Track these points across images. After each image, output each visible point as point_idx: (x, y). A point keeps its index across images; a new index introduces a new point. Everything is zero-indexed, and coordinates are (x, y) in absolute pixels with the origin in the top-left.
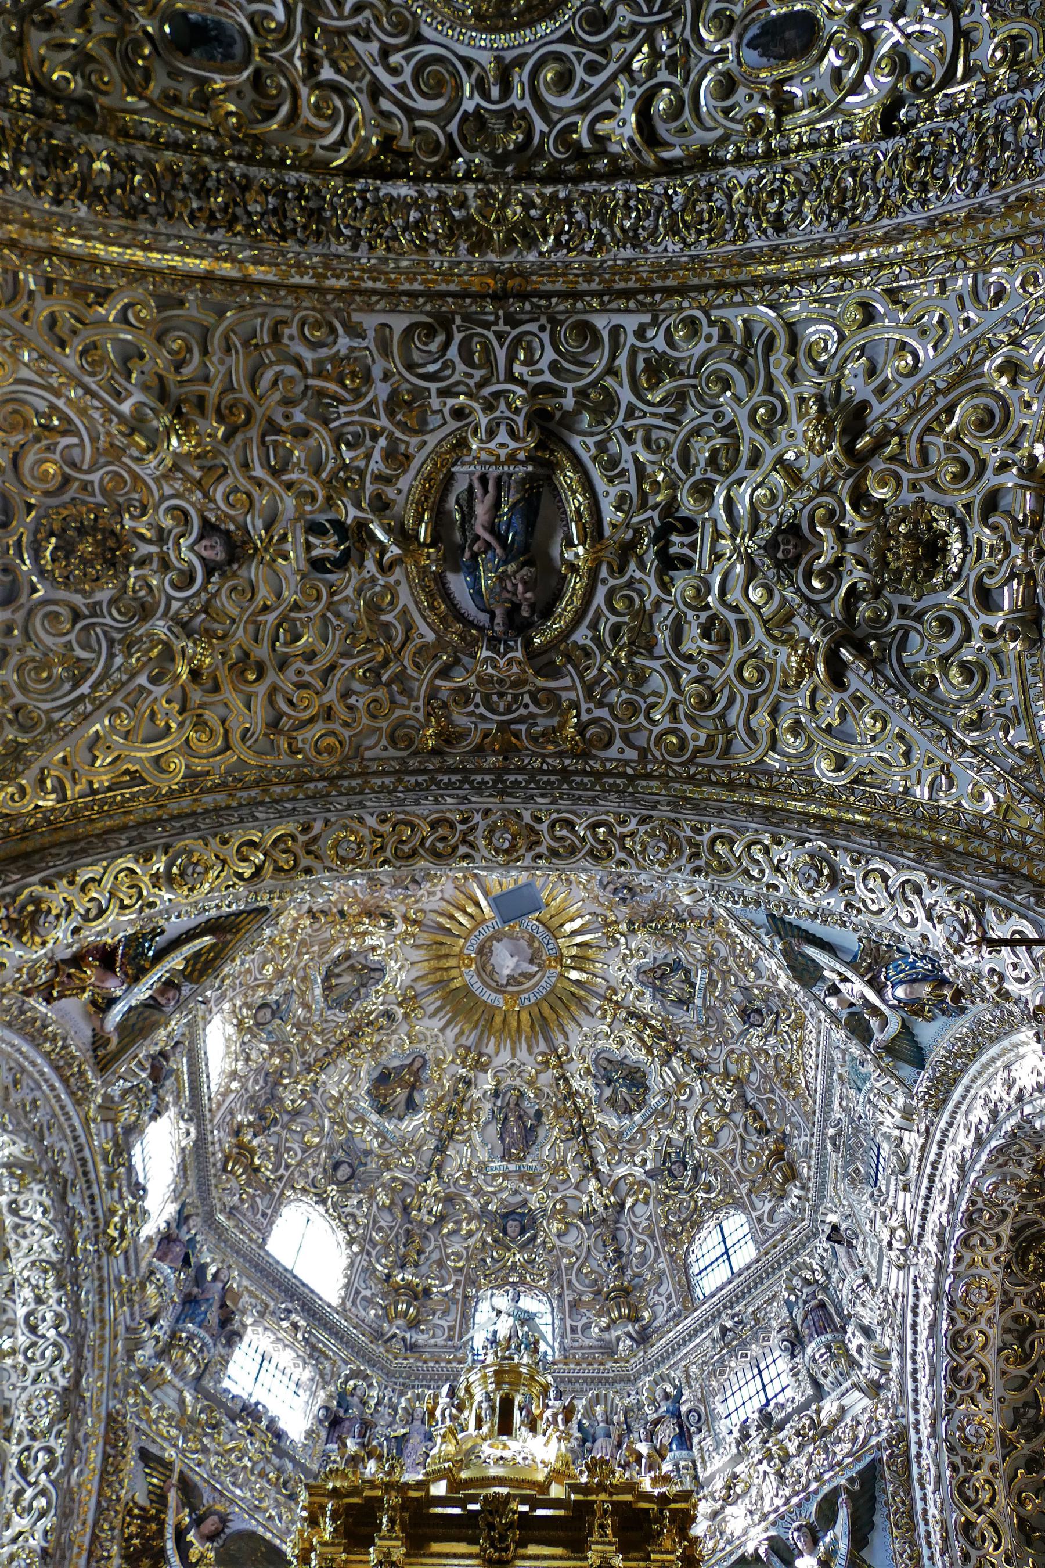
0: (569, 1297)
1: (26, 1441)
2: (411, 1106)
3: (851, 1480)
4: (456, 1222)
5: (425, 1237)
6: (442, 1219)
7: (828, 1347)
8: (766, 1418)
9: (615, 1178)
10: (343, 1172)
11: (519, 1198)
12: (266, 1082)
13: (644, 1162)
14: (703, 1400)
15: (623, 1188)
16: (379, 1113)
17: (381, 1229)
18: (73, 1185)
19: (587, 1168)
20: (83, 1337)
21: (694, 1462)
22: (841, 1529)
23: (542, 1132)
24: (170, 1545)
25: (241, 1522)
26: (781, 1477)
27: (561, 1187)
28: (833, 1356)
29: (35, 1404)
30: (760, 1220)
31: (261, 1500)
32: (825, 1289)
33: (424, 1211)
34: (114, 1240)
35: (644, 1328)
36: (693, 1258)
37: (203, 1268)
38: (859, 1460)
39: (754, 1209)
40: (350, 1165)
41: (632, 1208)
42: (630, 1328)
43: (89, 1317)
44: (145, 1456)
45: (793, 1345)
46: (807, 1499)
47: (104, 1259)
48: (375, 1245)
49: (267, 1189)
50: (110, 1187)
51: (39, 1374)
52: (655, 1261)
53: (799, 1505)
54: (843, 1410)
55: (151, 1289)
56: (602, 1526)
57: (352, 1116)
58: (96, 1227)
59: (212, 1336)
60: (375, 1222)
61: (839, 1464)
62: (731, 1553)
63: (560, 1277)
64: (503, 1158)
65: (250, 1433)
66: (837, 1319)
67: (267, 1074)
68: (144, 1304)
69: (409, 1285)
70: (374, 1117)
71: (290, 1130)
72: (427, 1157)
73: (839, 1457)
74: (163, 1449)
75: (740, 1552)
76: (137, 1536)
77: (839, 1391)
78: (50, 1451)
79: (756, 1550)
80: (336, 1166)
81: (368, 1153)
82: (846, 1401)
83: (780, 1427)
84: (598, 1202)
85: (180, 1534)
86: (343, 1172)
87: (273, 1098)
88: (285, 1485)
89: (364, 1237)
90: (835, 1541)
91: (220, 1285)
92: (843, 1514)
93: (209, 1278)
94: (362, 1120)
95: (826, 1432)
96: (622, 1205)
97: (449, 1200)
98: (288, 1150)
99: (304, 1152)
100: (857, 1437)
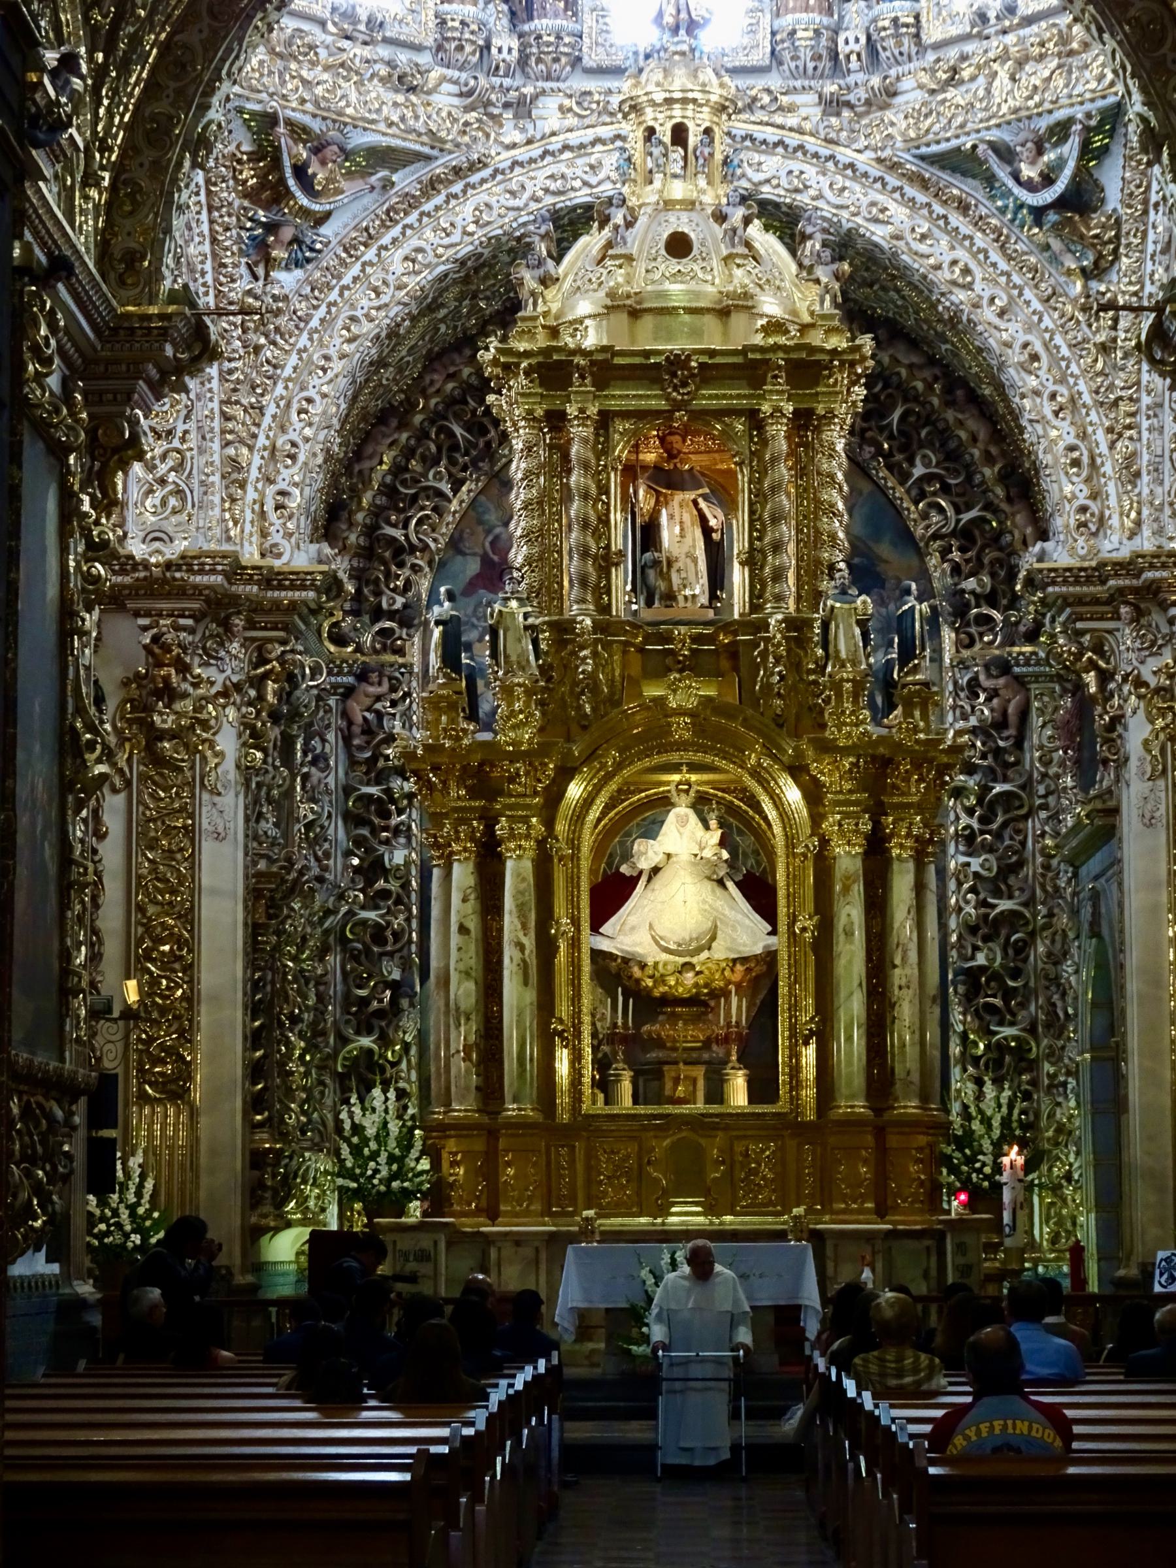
8: (1011, 10)
21: (917, 17)
22: (1071, 149)
24: (291, 182)
25: (359, 139)
26: (1013, 79)
31: (378, 111)
38: (1104, 97)
46: (1040, 115)
56: (776, 377)
62: (948, 140)
65: (347, 38)
75: (954, 143)
79: (974, 147)
83: (1029, 21)
85: (300, 171)
88: (400, 78)
90: (1061, 163)
95: (1071, 53)
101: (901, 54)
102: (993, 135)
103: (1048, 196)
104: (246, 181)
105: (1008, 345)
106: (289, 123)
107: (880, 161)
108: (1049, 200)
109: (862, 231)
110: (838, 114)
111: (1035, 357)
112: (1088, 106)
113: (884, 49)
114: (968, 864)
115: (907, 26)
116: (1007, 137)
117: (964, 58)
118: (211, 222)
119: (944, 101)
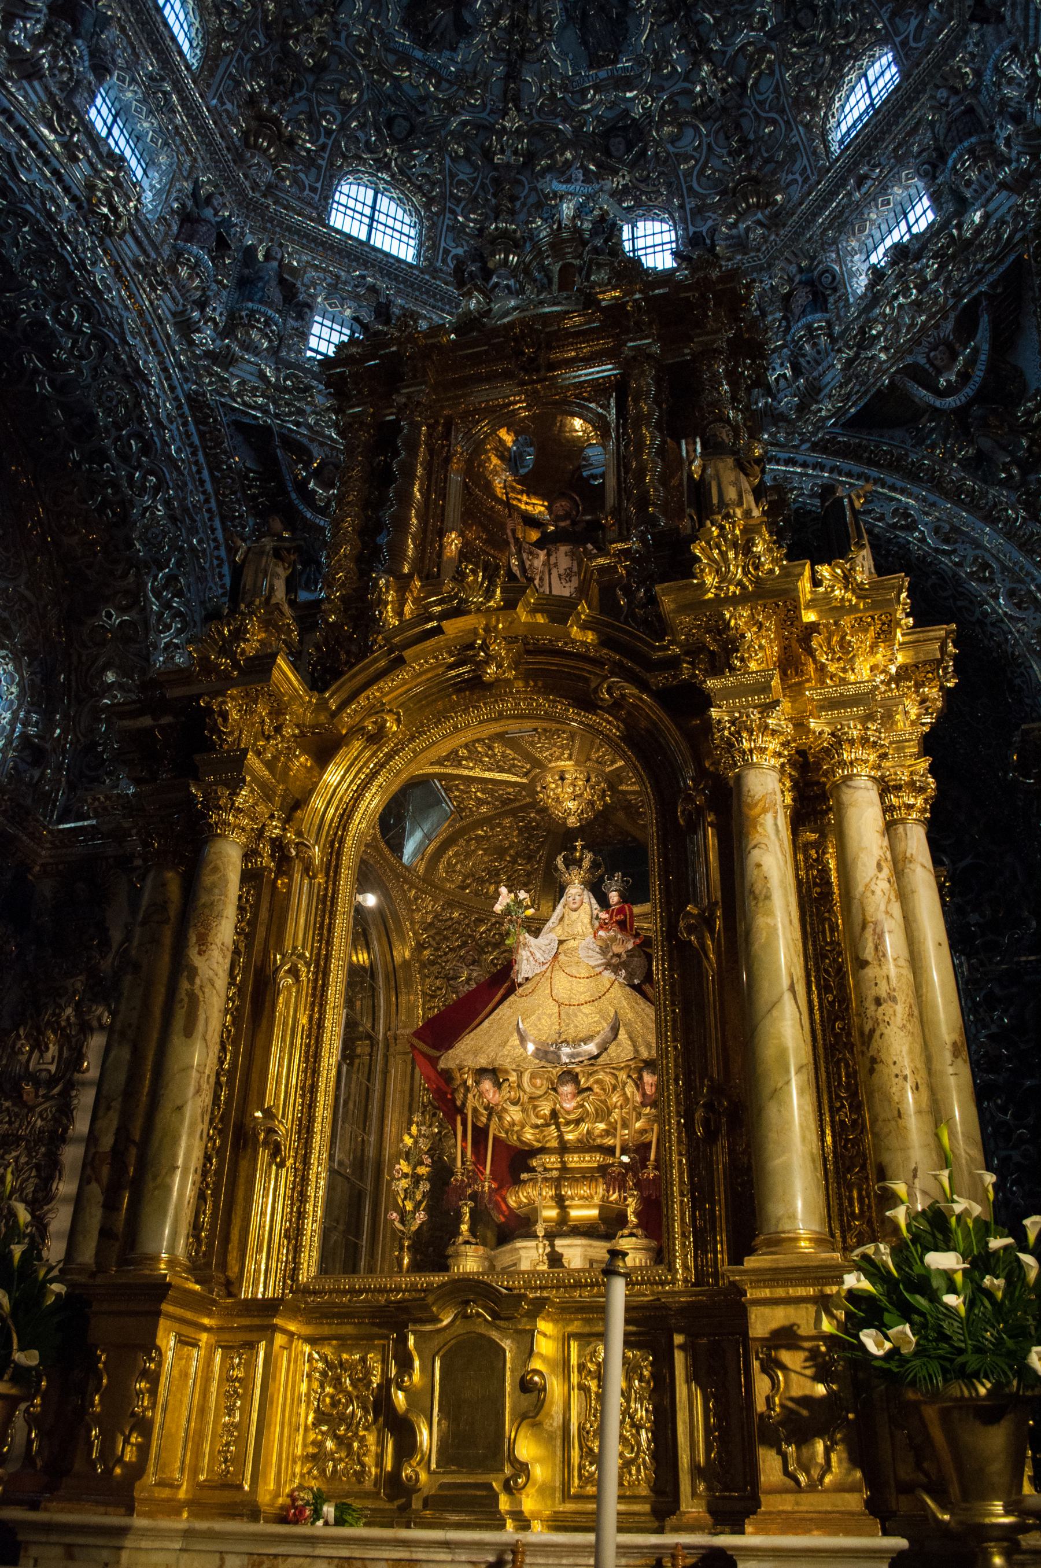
0: (691, 204)
1: (114, 433)
2: (464, 30)
3: (993, 286)
4: (551, 156)
5: (519, 182)
6: (531, 157)
7: (971, 151)
9: (731, 51)
10: (401, 126)
11: (617, 111)
12: (268, 36)
13: (764, 19)
14: (839, 260)
15: (742, 62)
16: (425, 48)
17: (461, 183)
18: (22, 160)
19: (694, 52)
20: (121, 324)
22: (982, 338)
23: (630, 21)
24: (294, 496)
27: (666, 84)
28: (976, 160)
29: (104, 397)
30: (904, 43)
32: (976, 90)
33: (508, 152)
34: (105, 216)
35: (777, 214)
36: (832, 122)
37: (251, 251)
38: (1001, 261)
39: (897, 35)
40: (403, 117)
41: (755, 84)
42: (760, 216)
43: (120, 306)
44: (240, 427)
45: (935, 167)
47: (108, 241)
48: (459, 200)
49: (310, 161)
50: (74, 159)
51: (95, 369)
52: (787, 137)
53: (937, 326)
54: (986, 217)
55: (184, 272)
57: (392, 58)
58: (79, 207)
59: (279, 312)
60: (452, 176)
61: (979, 272)
62: (866, 392)
63: (679, 188)
64: (591, 67)
66: (986, 120)
67: (267, 26)
68: (182, 287)
69: (505, 233)
70: (418, 54)
71: (319, 90)
72: (497, 90)
73: (980, 266)
74: (255, 418)
75: (874, 390)
76: (261, 495)
77: (983, 197)
78: (139, 436)
80: (390, 122)
81: (425, 98)
82: (991, 207)
84: (714, 89)
85: (301, 486)
86: (401, 126)
87: (287, 56)
89: (442, 196)
90: (976, 350)
91: (275, 264)
92: (985, 320)
93: (260, 257)
94: (405, 60)
96: (744, 85)
97: (535, 133)
98: (323, 115)
99: (344, 113)
100: (999, 237)
101: (819, 352)
102: (909, 360)
103: (969, 391)
104: (254, 497)
105: (959, 565)
106: (282, 436)
107: (815, 447)
108: (971, 393)
109: (809, 508)
110: (775, 425)
111: (985, 566)
112: (991, 279)
113: (804, 356)
114: (1009, 1158)
115: (820, 328)
116: (922, 361)
117: (868, 320)
118: (225, 529)
119: (860, 364)
